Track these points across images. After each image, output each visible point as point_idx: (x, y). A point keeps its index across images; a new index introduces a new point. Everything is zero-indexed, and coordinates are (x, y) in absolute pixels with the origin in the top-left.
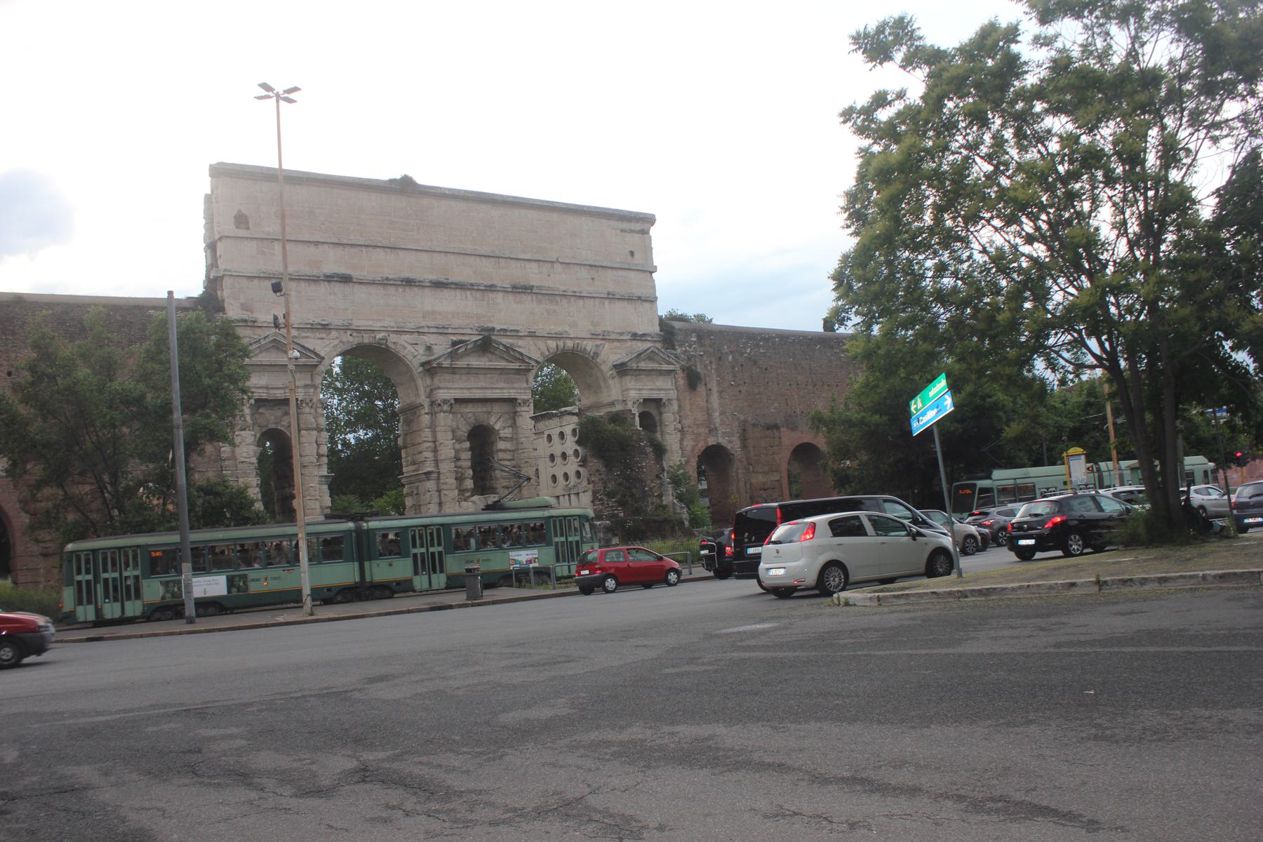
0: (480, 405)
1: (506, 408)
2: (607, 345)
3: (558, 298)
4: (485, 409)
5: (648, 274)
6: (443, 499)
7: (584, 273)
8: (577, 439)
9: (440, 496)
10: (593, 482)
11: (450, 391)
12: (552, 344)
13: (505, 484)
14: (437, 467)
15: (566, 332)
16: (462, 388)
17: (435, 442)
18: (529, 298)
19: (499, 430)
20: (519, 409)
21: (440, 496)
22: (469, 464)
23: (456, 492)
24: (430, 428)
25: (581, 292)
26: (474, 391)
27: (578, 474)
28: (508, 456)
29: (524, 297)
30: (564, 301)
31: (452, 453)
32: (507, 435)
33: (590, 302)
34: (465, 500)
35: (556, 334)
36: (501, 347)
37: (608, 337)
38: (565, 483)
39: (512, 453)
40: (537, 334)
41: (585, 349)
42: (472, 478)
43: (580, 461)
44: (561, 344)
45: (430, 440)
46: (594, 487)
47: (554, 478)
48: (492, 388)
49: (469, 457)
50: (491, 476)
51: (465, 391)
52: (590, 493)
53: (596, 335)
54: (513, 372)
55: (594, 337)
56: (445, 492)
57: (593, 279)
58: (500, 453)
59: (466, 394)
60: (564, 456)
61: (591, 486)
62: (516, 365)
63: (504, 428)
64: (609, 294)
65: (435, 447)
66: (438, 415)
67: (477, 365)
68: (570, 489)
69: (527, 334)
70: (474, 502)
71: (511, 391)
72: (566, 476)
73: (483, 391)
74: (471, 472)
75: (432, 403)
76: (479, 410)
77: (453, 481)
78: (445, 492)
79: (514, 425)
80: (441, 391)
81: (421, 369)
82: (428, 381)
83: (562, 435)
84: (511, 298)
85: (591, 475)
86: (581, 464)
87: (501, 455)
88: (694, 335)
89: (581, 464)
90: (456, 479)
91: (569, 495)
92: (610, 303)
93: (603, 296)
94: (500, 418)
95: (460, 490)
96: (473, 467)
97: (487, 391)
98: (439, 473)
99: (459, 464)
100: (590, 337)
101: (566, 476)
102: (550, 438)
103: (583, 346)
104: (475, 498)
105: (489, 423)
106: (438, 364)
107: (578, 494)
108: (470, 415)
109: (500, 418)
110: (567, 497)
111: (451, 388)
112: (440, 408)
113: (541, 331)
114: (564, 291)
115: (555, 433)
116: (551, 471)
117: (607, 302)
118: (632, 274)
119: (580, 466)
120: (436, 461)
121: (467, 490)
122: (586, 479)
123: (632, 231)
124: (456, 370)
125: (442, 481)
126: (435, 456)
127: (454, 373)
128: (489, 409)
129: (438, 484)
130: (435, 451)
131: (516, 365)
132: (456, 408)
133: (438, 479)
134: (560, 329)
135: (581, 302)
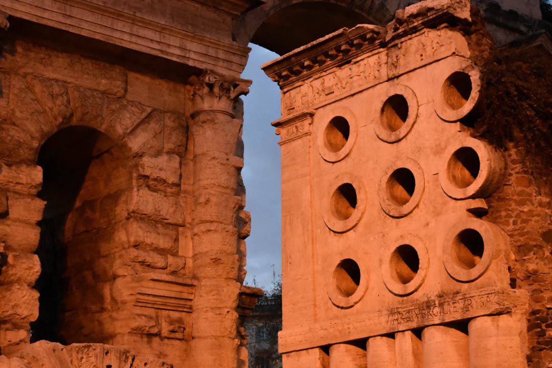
8: (468, 107)
10: (532, 277)
13: (141, 322)
19: (140, 155)
22: (33, 236)
32: (163, 175)
38: (398, 288)
43: (473, 197)
46: (536, 297)
48: (134, 21)
49: (38, 217)
50: (101, 299)
61: (522, 293)
63: (159, 153)
73: (108, 22)
79: (182, 152)
85: (522, 250)
86: (479, 204)
89: (479, 204)
91: (418, 332)
96: (41, 250)
104: (42, 346)
107: (462, 326)
110: (406, 341)
116: (339, 248)
119: (478, 213)
128: (117, 86)
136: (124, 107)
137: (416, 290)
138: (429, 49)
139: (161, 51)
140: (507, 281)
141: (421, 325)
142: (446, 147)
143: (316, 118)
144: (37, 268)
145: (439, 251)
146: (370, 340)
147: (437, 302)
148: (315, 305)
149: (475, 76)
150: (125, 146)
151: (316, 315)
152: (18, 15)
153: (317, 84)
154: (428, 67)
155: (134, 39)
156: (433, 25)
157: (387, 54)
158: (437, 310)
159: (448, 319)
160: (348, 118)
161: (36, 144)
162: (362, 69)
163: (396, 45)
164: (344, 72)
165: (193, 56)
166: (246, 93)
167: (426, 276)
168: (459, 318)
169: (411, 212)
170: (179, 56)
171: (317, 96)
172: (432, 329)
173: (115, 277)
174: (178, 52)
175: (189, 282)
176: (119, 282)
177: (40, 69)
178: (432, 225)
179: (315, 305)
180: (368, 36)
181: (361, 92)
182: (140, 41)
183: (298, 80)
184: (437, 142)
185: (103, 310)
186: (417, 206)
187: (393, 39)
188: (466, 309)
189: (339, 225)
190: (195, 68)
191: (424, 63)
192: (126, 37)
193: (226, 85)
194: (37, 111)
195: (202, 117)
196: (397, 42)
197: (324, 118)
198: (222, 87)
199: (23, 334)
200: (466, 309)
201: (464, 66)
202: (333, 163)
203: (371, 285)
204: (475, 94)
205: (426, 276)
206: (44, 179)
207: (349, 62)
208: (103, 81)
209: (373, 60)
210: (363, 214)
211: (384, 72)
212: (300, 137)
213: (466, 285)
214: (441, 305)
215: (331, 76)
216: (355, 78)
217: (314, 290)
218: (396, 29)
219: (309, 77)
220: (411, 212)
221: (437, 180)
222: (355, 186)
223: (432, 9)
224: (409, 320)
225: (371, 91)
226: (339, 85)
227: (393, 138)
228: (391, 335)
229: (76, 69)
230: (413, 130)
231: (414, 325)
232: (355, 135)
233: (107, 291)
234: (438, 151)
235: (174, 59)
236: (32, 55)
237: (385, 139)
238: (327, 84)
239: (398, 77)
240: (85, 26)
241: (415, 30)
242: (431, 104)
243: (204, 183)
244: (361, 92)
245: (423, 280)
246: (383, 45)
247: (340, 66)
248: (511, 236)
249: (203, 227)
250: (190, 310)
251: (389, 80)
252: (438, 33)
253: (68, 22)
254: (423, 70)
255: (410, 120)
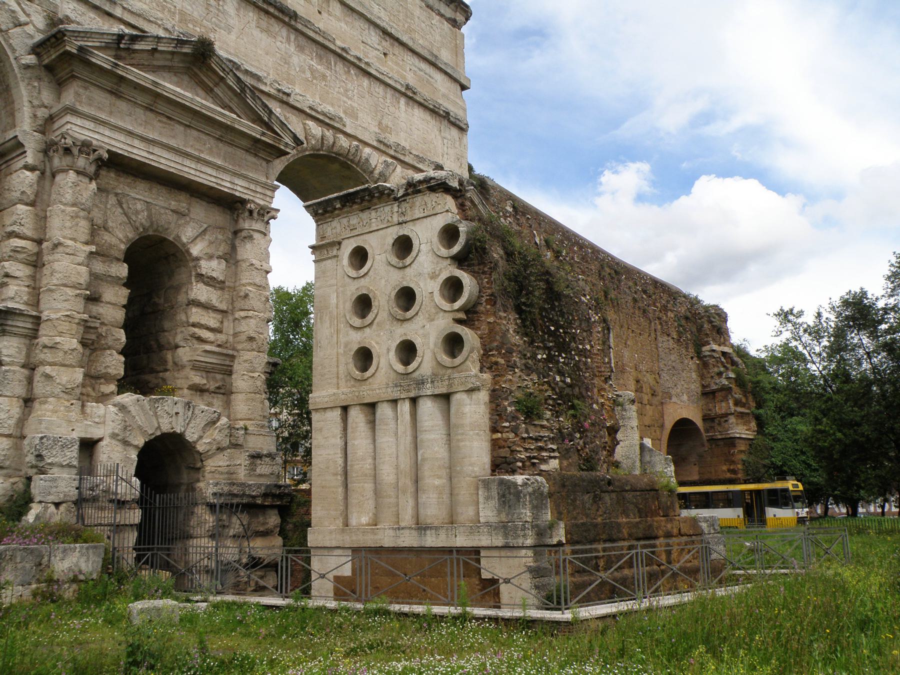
0: (163, 190)
1: (217, 217)
2: (399, 168)
3: (332, 59)
4: (174, 204)
5: (459, 88)
6: (40, 387)
7: (374, 37)
8: (456, 249)
9: (30, 381)
11: (101, 129)
12: (316, 130)
14: (36, 304)
15: (341, 118)
16: (130, 133)
17: (39, 242)
18: (284, 32)
19: (198, 259)
20: (246, 225)
21: (30, 381)
22: (120, 315)
23: (78, 375)
24: (32, 204)
25: (367, 64)
26: (157, 150)
27: (453, 343)
28: (211, 320)
29: (276, 27)
30: (340, 67)
31: (82, 274)
32: (214, 275)
33: (379, 90)
34: (103, 398)
35: (324, 114)
36: (231, 81)
37: (402, 158)
38: (400, 368)
39: (219, 316)
40: (291, 100)
41: (367, 160)
42: (122, 352)
43: (458, 310)
44: (329, 134)
45: (29, 233)
47: (364, 357)
48: (199, 160)
49: (124, 301)
50: (165, 362)
51: (136, 143)
52: (483, 396)
53: (385, 144)
54: (245, 143)
55: (382, 147)
56: (48, 369)
57: (385, 54)
58: (194, 310)
59: (139, 152)
60: (407, 297)
62: (254, 130)
63: (210, 257)
64: (408, 87)
65: (39, 254)
66: (59, 178)
67: (175, 93)
68: (421, 383)
69: (273, 92)
70: (122, 408)
71: (237, 181)
72: (408, 351)
74: (122, 336)
75: (47, 150)
76: (162, 204)
77: (74, 343)
78: (48, 369)
80: (79, 121)
81: (31, 59)
82: (47, 96)
83: (404, 246)
84: (251, 14)
86: (462, 316)
87: (196, 315)
88: (509, 203)
89: (462, 316)
90: (84, 343)
91: (414, 401)
92: (407, 104)
93: (399, 87)
94: (205, 231)
95: (86, 375)
96: (128, 326)
97: (187, 162)
98: (37, 320)
99: (96, 309)
100: (375, 144)
101: (408, 351)
102: (360, 256)
103: (364, 155)
104: (128, 398)
105: (178, 237)
106: (81, 49)
107: (446, 398)
108: (139, 206)
109: (204, 232)
110: (405, 407)
111: (103, 123)
112: (68, 160)
113: (299, 98)
114: (343, 49)
115: (434, 200)
116: (356, 339)
117: (403, 101)
118: (439, 77)
119: (459, 321)
120: (36, 295)
121: (106, 378)
122: (475, 356)
123: (442, 16)
124: (123, 89)
125: (43, 340)
126: (33, 278)
127: (116, 94)
128: (183, 206)
129: (30, 349)
130: (36, 263)
131: (254, 130)
132: (110, 178)
133: (34, 335)
134: (328, 108)
135: (366, 82)
136: (187, 223)
137: (414, 371)
138: (429, 205)
139: (217, 184)
140: (478, 368)
141: (417, 395)
142: (439, 275)
143: (342, 246)
144: (124, 339)
145: (432, 346)
146: (379, 404)
147: (429, 380)
148: (338, 378)
149: (463, 228)
150: (188, 251)
151: (338, 384)
152: (114, 149)
153: (345, 221)
154: (429, 219)
155: (198, 174)
156: (432, 189)
157: (398, 206)
158: (429, 385)
159: (437, 391)
160: (367, 247)
161: (123, 247)
162: (378, 214)
163: (405, 200)
164: (365, 215)
165: (239, 188)
166: (274, 218)
167: (421, 362)
168: (445, 392)
169: (412, 317)
170: (229, 188)
171: (343, 230)
172: (425, 399)
173: (177, 347)
174: (228, 185)
175: (230, 352)
176: (180, 351)
177: (127, 190)
178: (427, 326)
179: (338, 378)
180: (386, 192)
181: (378, 230)
182: (202, 175)
183: (330, 217)
184: (433, 271)
185: (166, 370)
186: (417, 314)
187: (403, 196)
188: (450, 385)
189: (357, 322)
190: (240, 197)
191: (425, 215)
192: (193, 172)
193: (262, 212)
194: (124, 222)
195: (244, 234)
196: (405, 198)
197: (348, 247)
198: (259, 213)
199: (113, 387)
200: (450, 385)
201: (455, 220)
202: (354, 278)
203: (381, 365)
204: (462, 240)
205: (421, 362)
206: (129, 273)
207: (369, 208)
208: (173, 203)
209: (387, 209)
210: (376, 316)
211: (395, 219)
212: (330, 258)
213: (450, 371)
214: (432, 382)
215: (355, 216)
216: (374, 220)
217: (338, 366)
218: (406, 190)
219: (338, 215)
220: (412, 317)
221: (432, 297)
222: (371, 296)
223: (434, 178)
224: (409, 391)
225: (384, 230)
226: (361, 224)
227: (401, 265)
228: (395, 402)
229: (154, 192)
230: (415, 262)
231: (412, 394)
232: (372, 260)
233: (169, 356)
234: (433, 276)
235: (226, 190)
236: (122, 179)
237: (395, 265)
238: (351, 222)
239: (405, 223)
240: (163, 161)
241: (419, 191)
242: (429, 244)
243: (244, 281)
244: (378, 230)
245: (419, 366)
246: (396, 199)
247: (362, 211)
248: (481, 338)
249: (243, 314)
250: (230, 373)
251: (399, 224)
252: (437, 195)
253: (151, 157)
254: (425, 219)
255: (413, 254)
